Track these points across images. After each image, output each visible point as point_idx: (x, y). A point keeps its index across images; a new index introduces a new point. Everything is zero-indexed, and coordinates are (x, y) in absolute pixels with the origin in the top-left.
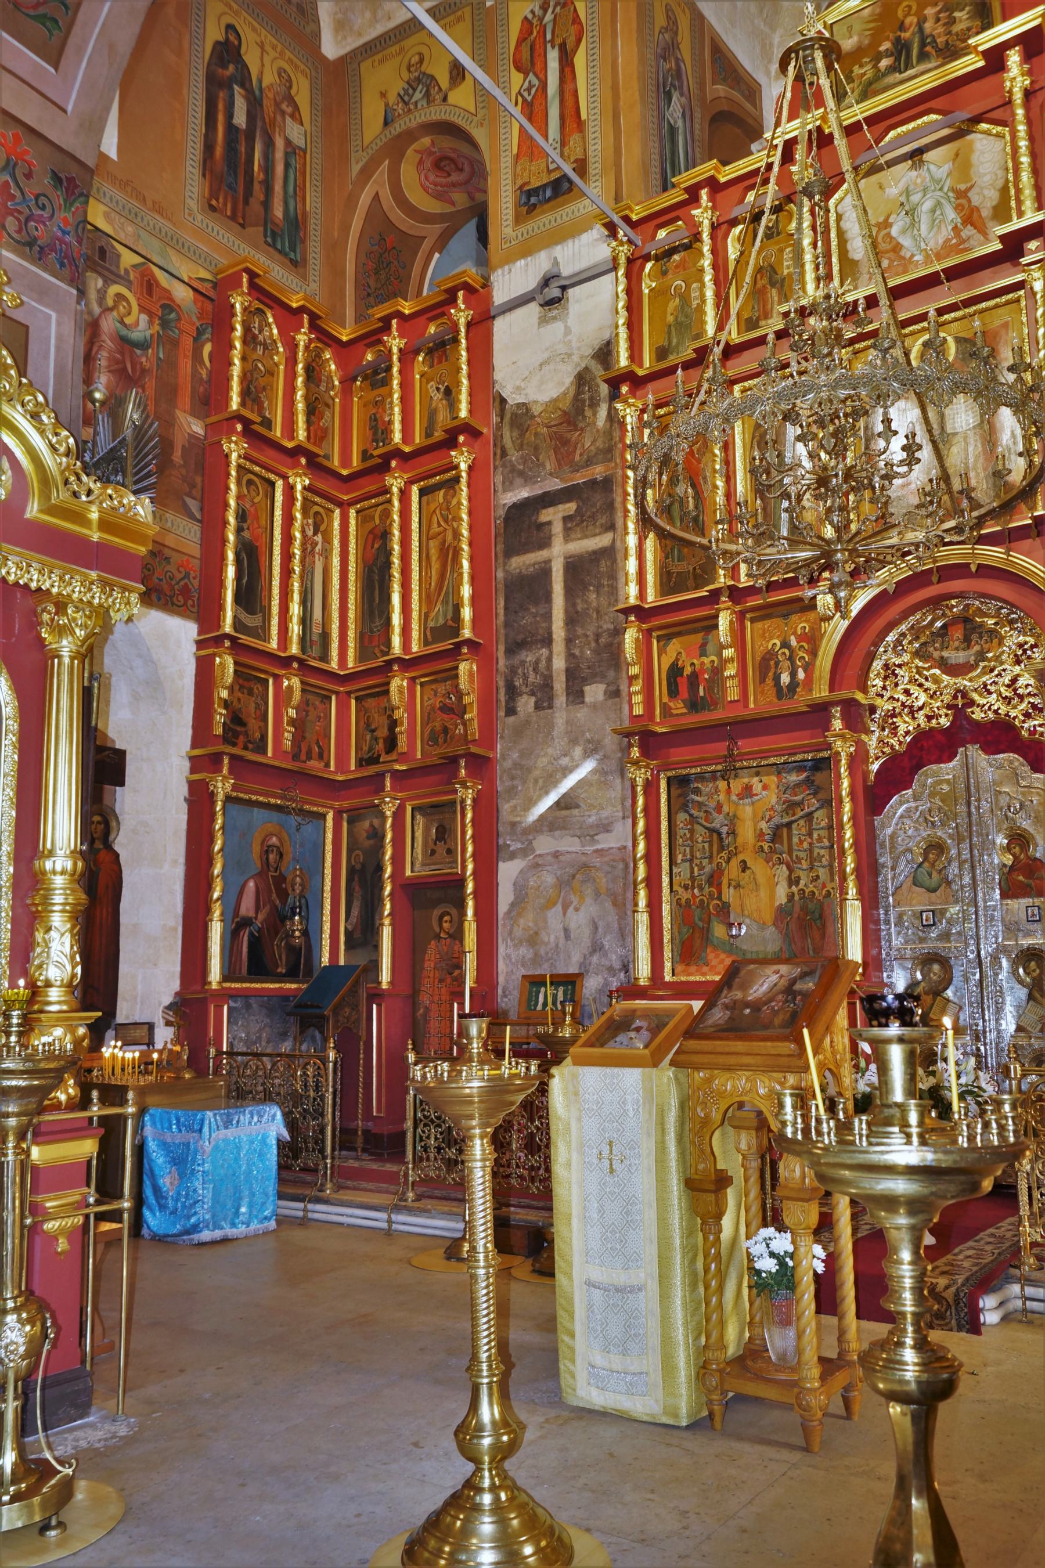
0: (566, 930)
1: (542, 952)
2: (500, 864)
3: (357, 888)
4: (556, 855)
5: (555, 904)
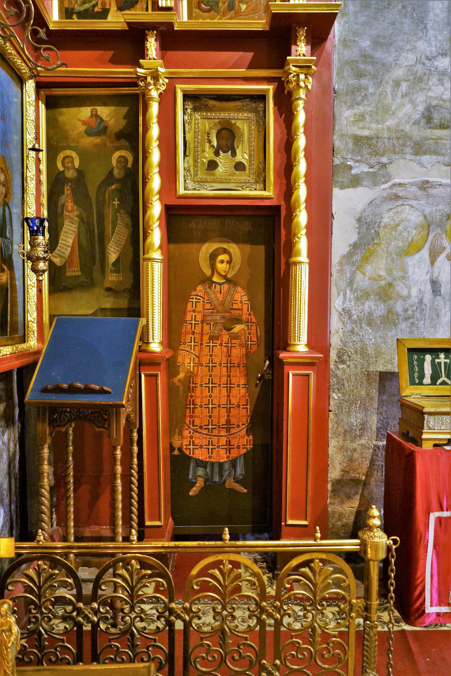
0: (435, 285)
1: (399, 308)
2: (336, 192)
3: (70, 205)
4: (424, 186)
5: (419, 250)
